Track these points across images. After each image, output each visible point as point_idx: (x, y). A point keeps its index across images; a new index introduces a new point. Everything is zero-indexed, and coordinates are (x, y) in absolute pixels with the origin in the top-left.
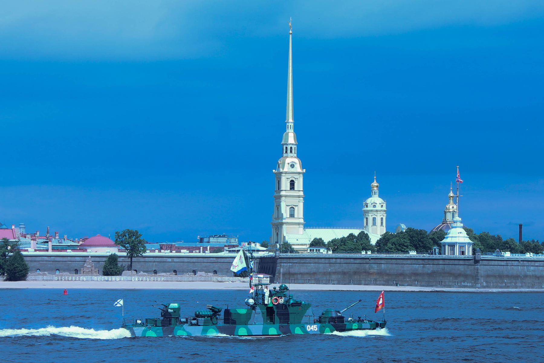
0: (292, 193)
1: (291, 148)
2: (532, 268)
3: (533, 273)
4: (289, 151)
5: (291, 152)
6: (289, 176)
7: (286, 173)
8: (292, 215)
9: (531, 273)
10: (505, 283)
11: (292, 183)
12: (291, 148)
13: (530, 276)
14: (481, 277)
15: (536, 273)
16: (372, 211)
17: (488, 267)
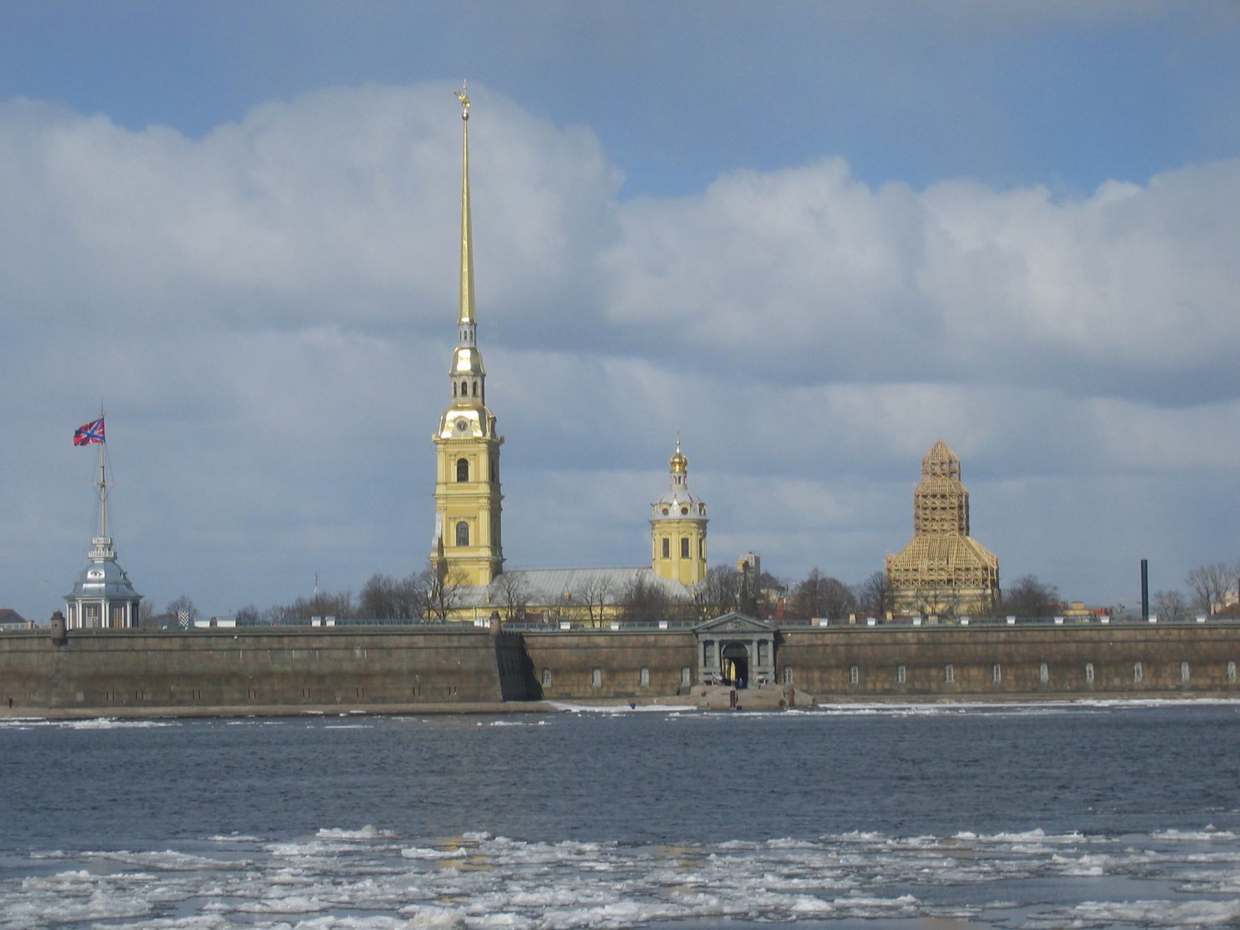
0: (463, 489)
1: (464, 384)
2: (295, 654)
3: (299, 667)
4: (470, 390)
5: (464, 392)
6: (452, 449)
7: (446, 442)
8: (463, 540)
9: (289, 669)
10: (172, 695)
11: (463, 467)
12: (464, 384)
13: (284, 675)
14: (69, 679)
15: (314, 667)
16: (659, 521)
17: (102, 656)
